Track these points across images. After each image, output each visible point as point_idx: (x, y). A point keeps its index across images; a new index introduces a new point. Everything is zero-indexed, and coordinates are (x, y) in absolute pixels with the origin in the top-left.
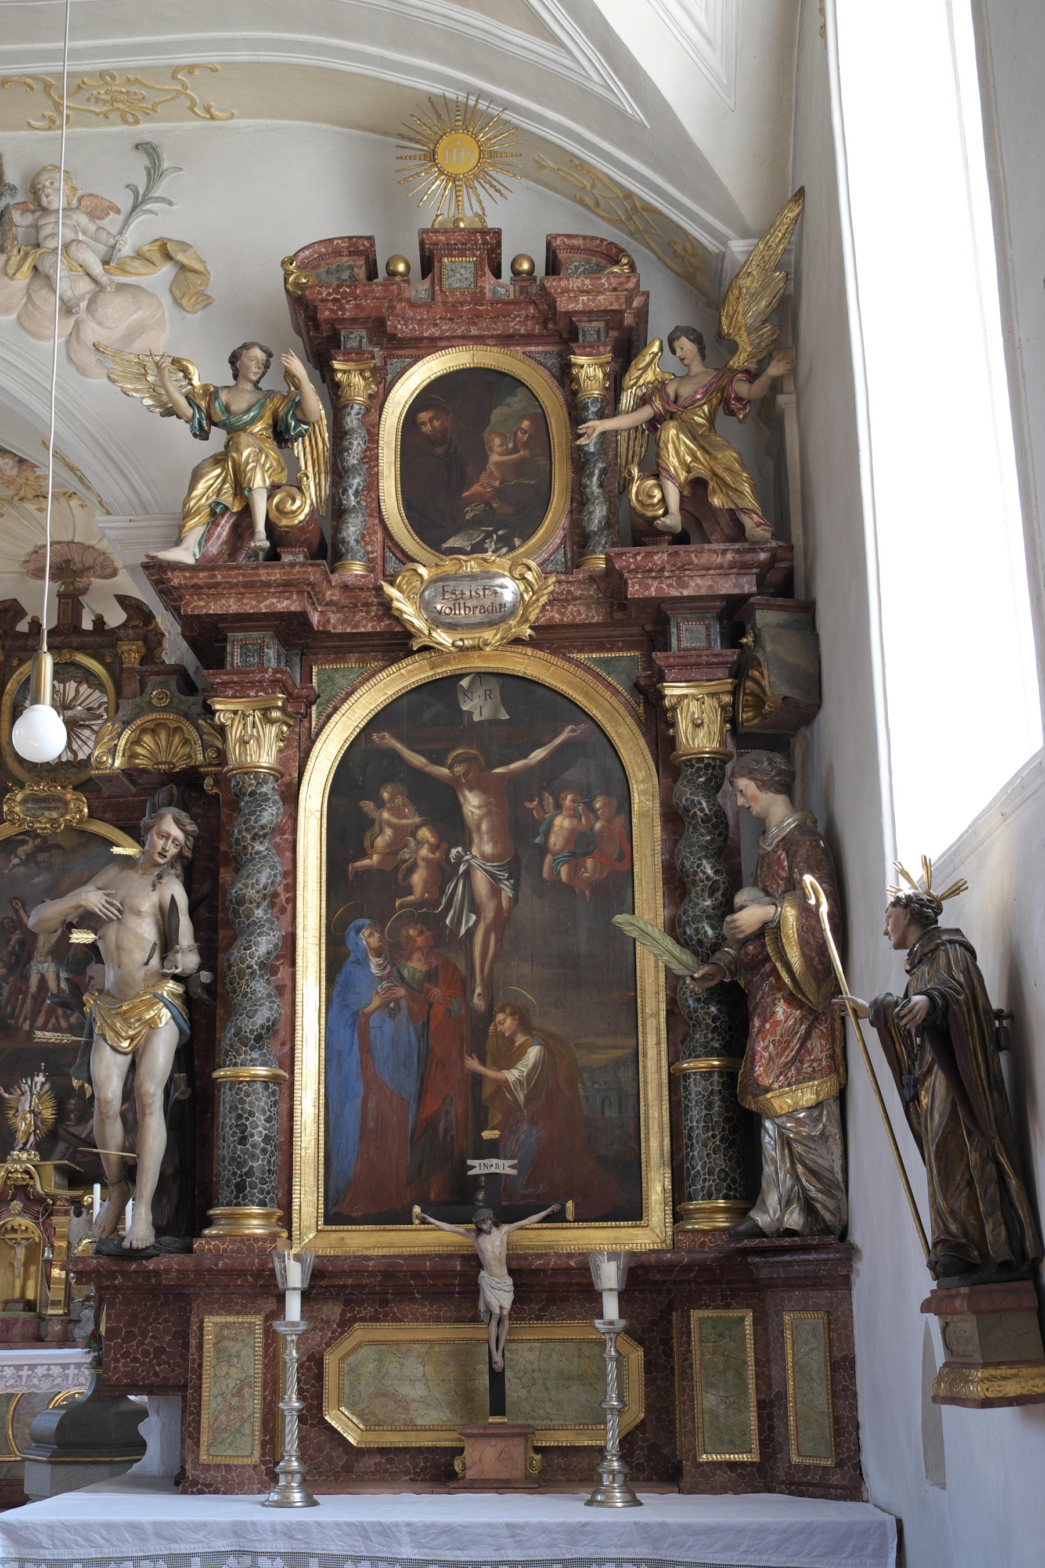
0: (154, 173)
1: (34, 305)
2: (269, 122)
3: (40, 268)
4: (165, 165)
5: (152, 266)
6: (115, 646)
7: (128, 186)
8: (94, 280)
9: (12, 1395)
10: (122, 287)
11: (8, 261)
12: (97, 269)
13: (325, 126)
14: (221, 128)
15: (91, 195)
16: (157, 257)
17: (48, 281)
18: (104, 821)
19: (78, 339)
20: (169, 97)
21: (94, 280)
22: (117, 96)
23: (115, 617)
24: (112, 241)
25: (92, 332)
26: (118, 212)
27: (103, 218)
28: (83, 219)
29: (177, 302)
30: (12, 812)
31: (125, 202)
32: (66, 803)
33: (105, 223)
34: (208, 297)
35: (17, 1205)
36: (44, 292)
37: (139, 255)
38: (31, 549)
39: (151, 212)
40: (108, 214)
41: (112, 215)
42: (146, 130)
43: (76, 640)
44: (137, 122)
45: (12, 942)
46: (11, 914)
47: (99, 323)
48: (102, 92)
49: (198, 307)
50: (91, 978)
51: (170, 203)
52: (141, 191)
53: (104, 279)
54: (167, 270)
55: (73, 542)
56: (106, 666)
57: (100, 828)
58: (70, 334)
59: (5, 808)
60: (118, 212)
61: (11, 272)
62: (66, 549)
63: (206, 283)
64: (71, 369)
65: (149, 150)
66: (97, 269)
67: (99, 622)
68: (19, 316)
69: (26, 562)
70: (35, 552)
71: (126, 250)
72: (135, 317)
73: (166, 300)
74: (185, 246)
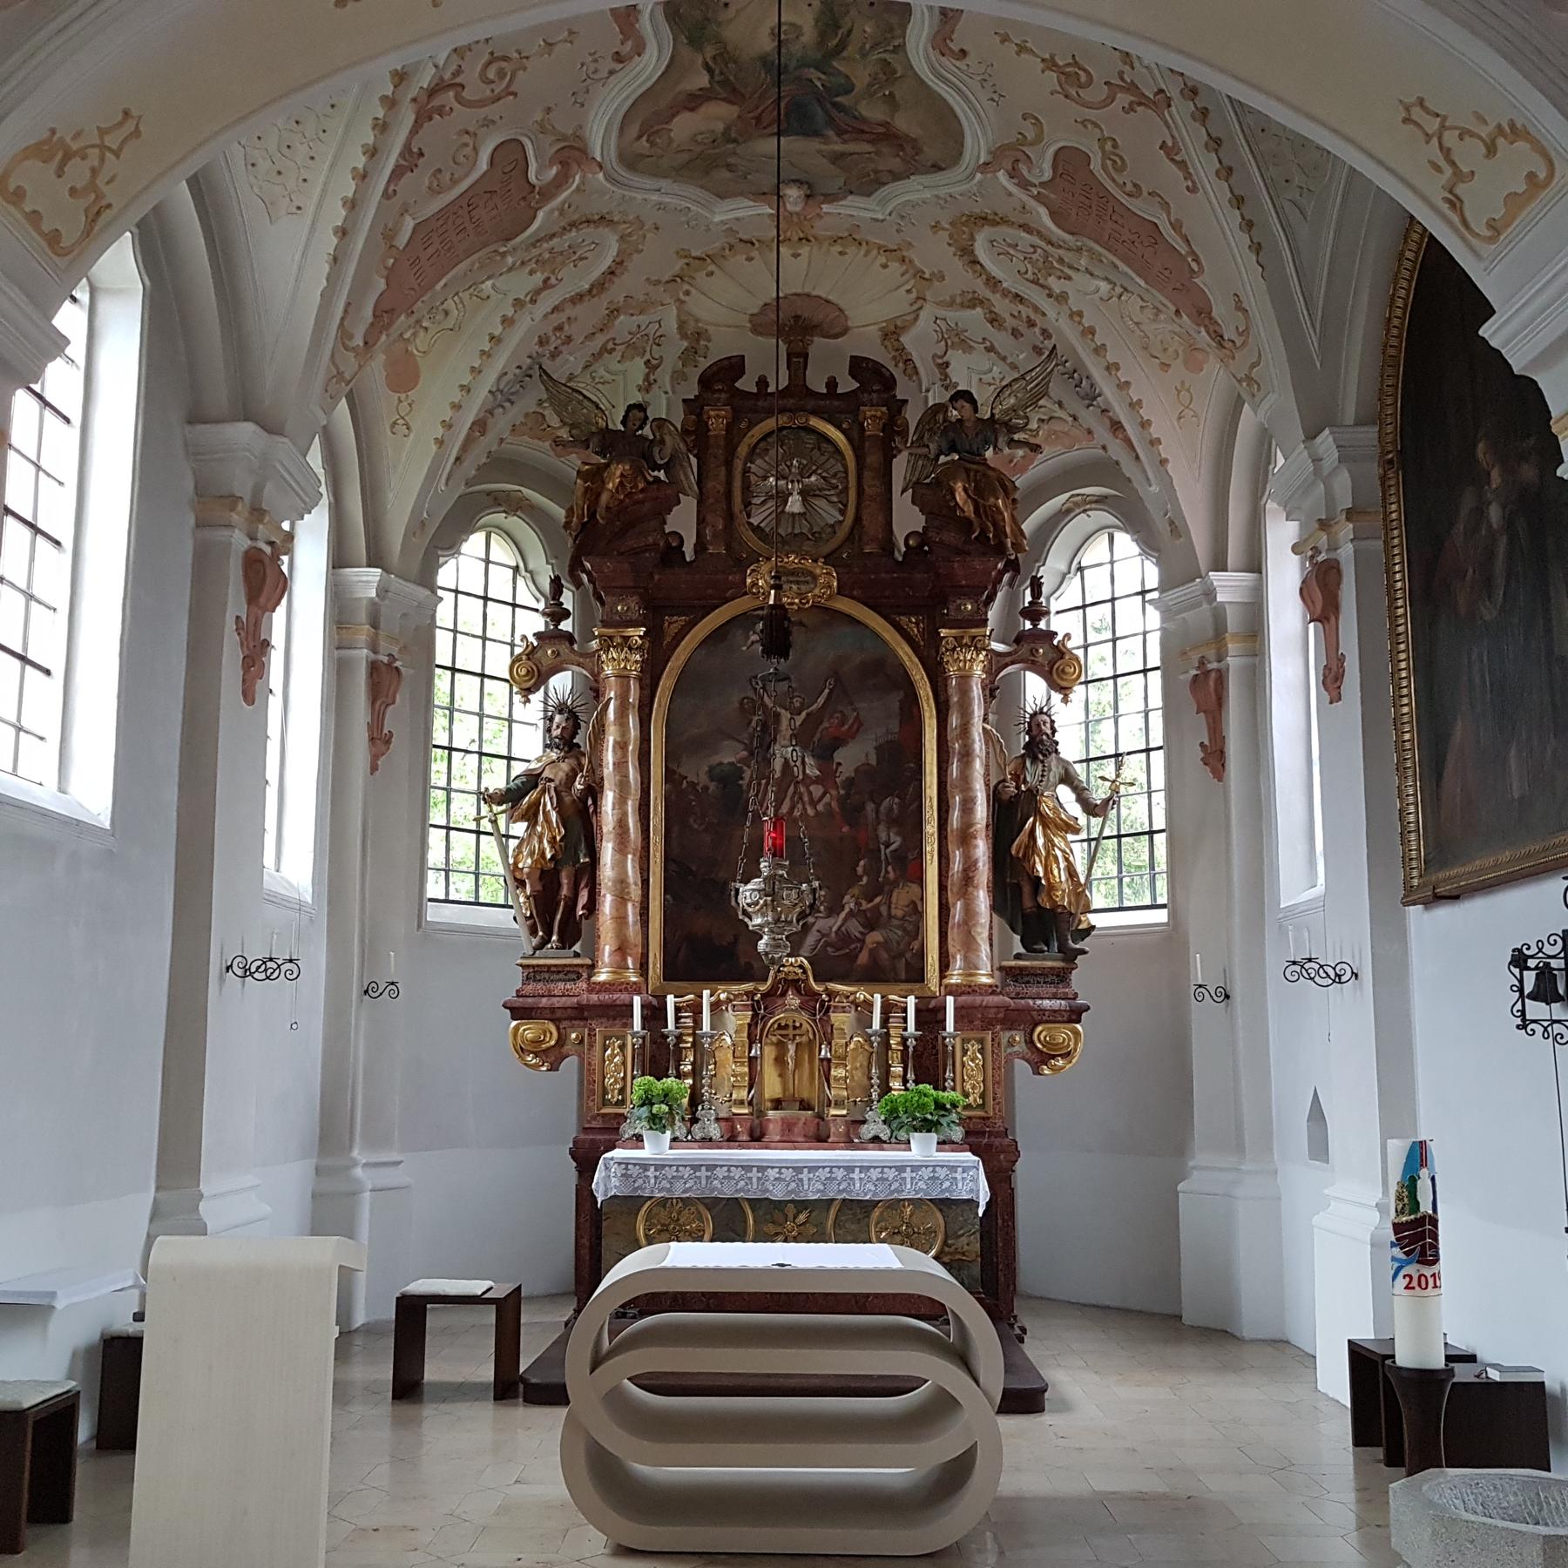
6: (855, 412)
9: (833, 1200)
18: (853, 598)
23: (847, 385)
30: (755, 584)
32: (815, 578)
35: (793, 1000)
43: (811, 404)
45: (754, 724)
46: (751, 694)
50: (839, 764)
56: (843, 432)
57: (845, 605)
59: (749, 581)
67: (832, 384)
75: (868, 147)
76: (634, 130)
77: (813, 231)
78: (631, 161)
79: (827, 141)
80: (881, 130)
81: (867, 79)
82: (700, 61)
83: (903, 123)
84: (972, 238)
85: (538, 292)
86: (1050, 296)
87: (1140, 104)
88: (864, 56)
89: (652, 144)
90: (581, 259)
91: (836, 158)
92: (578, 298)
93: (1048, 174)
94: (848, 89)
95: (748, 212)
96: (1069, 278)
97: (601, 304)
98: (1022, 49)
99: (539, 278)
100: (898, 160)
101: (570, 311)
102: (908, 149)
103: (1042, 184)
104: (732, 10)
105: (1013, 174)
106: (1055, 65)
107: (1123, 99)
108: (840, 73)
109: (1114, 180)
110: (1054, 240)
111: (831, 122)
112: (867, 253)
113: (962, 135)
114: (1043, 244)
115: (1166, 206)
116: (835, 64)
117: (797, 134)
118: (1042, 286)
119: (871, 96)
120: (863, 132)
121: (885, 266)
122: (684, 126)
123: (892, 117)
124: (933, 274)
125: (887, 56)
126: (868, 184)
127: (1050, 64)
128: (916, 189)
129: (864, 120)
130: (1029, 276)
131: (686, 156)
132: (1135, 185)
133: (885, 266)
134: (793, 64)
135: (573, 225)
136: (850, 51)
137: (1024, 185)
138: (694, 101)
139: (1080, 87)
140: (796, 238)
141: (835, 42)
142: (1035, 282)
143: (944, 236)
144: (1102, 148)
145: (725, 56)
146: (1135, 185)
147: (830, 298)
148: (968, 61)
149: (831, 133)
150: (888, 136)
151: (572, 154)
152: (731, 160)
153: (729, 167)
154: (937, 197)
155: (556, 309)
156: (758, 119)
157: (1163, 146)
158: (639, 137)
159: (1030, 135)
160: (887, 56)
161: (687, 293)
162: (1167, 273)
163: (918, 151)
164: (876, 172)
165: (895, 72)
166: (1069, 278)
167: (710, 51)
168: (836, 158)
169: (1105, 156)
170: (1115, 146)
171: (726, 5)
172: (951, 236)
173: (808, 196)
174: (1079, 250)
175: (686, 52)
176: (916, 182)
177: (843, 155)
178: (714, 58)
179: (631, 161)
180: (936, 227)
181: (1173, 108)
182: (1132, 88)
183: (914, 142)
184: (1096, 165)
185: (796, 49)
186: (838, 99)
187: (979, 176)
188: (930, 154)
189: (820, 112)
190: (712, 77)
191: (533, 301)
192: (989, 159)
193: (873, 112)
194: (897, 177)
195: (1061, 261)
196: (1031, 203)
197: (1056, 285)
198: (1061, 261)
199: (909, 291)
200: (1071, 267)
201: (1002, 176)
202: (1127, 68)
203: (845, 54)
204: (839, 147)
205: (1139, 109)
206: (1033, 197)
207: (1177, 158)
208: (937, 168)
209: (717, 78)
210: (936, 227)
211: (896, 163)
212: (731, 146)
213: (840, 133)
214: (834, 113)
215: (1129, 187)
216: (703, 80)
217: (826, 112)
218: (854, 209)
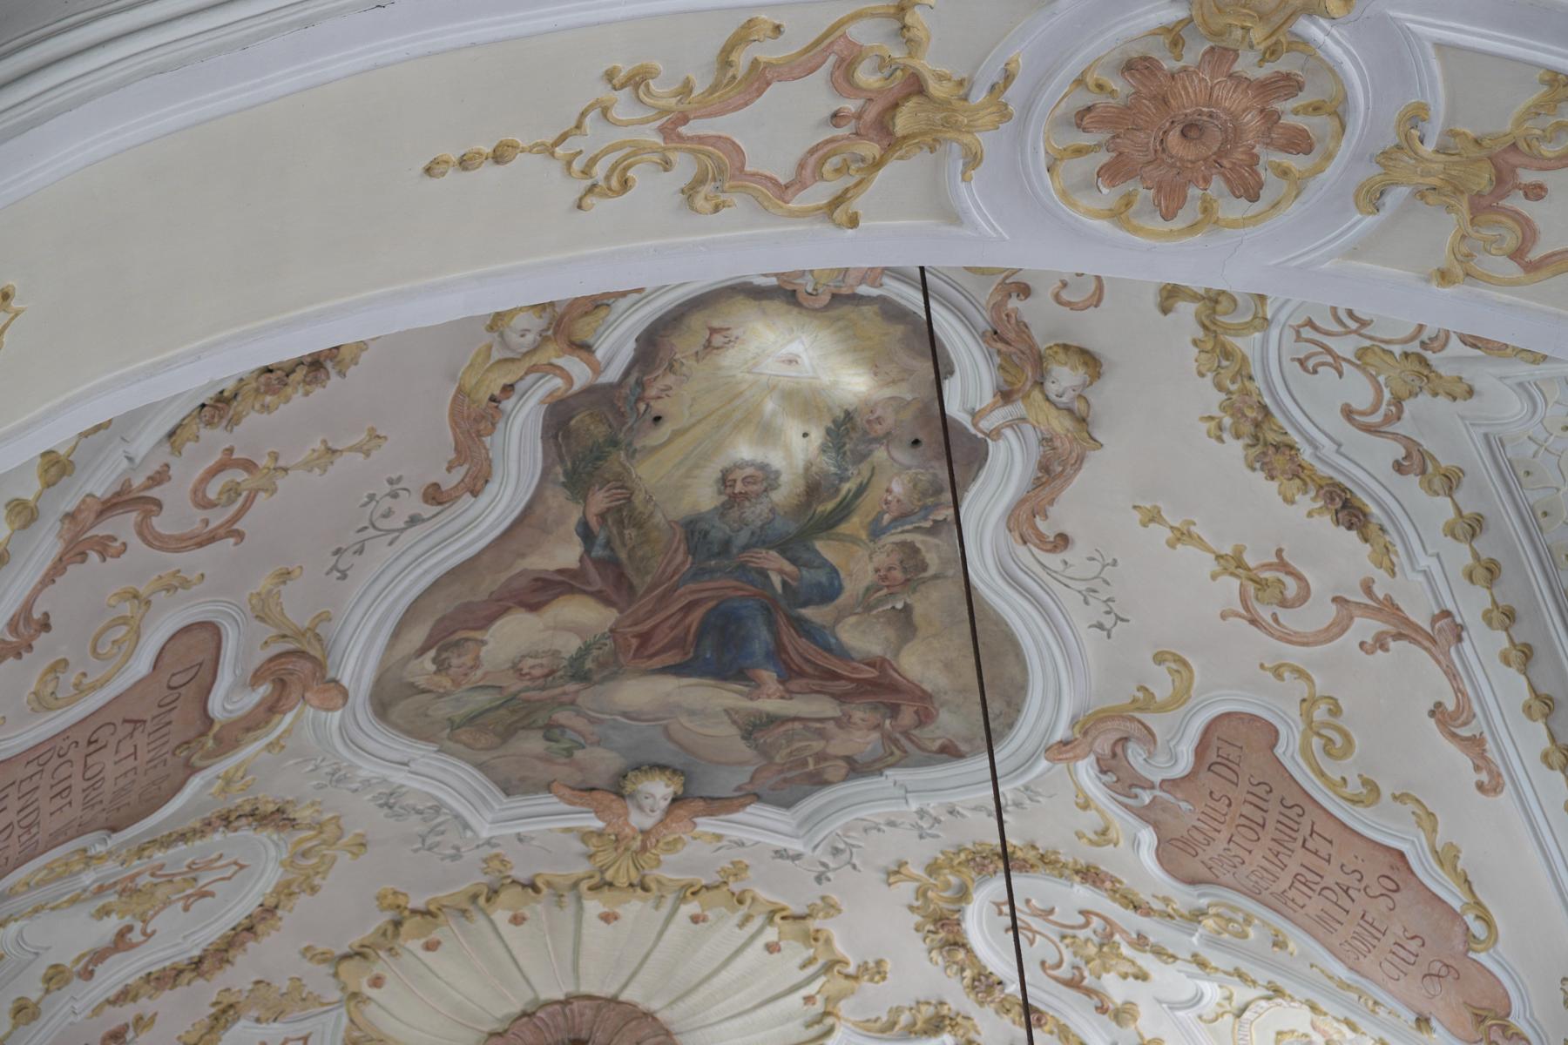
38: (516, 1007)
55: (613, 1001)
62: (589, 1013)
69: (492, 1035)
70: (524, 1014)
76: (417, 635)
77: (657, 872)
78: (390, 699)
80: (870, 673)
81: (869, 578)
82: (575, 516)
83: (915, 665)
84: (963, 894)
85: (99, 956)
86: (1102, 1009)
87: (1399, 636)
88: (876, 531)
89: (441, 666)
90: (203, 895)
91: (754, 727)
92: (168, 978)
94: (828, 592)
95: (550, 828)
96: (1142, 976)
97: (203, 994)
98: (1183, 535)
99: (113, 924)
100: (875, 735)
101: (145, 1006)
103: (1171, 784)
104: (666, 430)
106: (1240, 564)
107: (1366, 627)
108: (825, 564)
109: (1321, 774)
110: (1144, 896)
111: (778, 656)
115: (1428, 820)
116: (819, 545)
117: (702, 674)
118: (1089, 992)
119: (869, 609)
120: (835, 676)
121: (771, 948)
122: (514, 637)
123: (897, 653)
124: (864, 967)
125: (917, 539)
127: (1233, 563)
129: (843, 654)
130: (1065, 972)
131: (482, 700)
132: (1366, 782)
133: (771, 948)
134: (743, 538)
135: (227, 820)
136: (854, 525)
137: (1124, 782)
138: (540, 592)
139: (1283, 603)
140: (622, 881)
141: (830, 506)
142: (1074, 984)
143: (906, 890)
144: (1307, 716)
145: (624, 514)
146: (1366, 782)
147: (654, 1005)
148: (1066, 555)
149: (768, 676)
150: (882, 688)
151: (296, 670)
152: (562, 717)
153: (551, 731)
155: (125, 995)
156: (645, 638)
157: (1437, 711)
158: (422, 651)
159: (1162, 688)
160: (917, 539)
161: (377, 982)
162: (1413, 946)
165: (925, 568)
166: (1142, 976)
167: (599, 500)
168: (754, 727)
169: (1311, 728)
170: (1335, 710)
171: (657, 419)
172: (922, 893)
174: (1197, 916)
175: (557, 499)
177: (773, 720)
178: (602, 516)
179: (390, 699)
180: (895, 872)
181: (1466, 645)
182: (1388, 609)
184: (1288, 749)
185: (756, 512)
186: (808, 612)
187: (1044, 764)
188: (953, 722)
189: (764, 634)
190: (588, 551)
191: (88, 974)
193: (862, 638)
194: (856, 769)
195: (1141, 942)
197: (1116, 988)
198: (1141, 942)
199: (809, 1000)
200: (1159, 952)
201: (1085, 771)
202: (1380, 575)
203: (844, 528)
204: (771, 704)
205: (1392, 644)
207: (1464, 732)
209: (598, 552)
210: (895, 872)
211: (863, 742)
212: (572, 687)
213: (789, 673)
214: (789, 636)
215: (1355, 787)
216: (567, 554)
217: (776, 636)
218: (760, 828)
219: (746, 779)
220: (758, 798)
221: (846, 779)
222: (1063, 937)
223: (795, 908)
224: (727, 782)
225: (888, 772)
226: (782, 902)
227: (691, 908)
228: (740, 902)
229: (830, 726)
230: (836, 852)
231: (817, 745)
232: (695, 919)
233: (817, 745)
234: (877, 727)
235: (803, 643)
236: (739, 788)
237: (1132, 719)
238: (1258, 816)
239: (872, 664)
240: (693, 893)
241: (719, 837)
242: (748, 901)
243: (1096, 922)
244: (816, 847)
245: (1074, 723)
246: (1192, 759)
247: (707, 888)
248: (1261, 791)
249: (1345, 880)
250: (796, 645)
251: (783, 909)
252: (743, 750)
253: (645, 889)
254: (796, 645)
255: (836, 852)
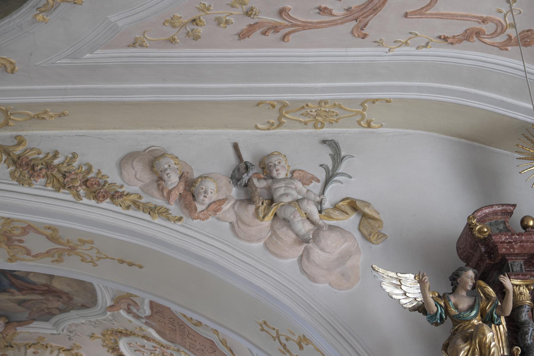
0: (337, 158)
1: (278, 237)
2: (401, 130)
3: (278, 214)
4: (343, 154)
5: (346, 215)
7: (321, 165)
8: (313, 222)
10: (331, 228)
11: (257, 209)
12: (316, 216)
13: (435, 134)
14: (372, 132)
15: (300, 170)
16: (348, 209)
17: (287, 223)
19: (308, 258)
20: (350, 115)
21: (313, 222)
22: (320, 113)
24: (318, 199)
25: (317, 254)
26: (318, 181)
27: (308, 185)
28: (299, 185)
29: (366, 238)
31: (322, 175)
33: (311, 187)
34: (385, 235)
36: (285, 229)
37: (335, 207)
39: (340, 182)
40: (311, 182)
41: (314, 182)
42: (328, 132)
44: (322, 127)
47: (322, 250)
48: (314, 110)
49: (379, 240)
51: (350, 177)
52: (331, 168)
53: (321, 222)
54: (354, 218)
58: (301, 256)
60: (318, 181)
61: (261, 216)
63: (381, 226)
64: (304, 277)
65: (333, 145)
66: (316, 216)
68: (265, 244)
71: (327, 205)
72: (344, 246)
73: (357, 235)
74: (368, 204)
75: (40, 297)
79: (12, 294)
80: (46, 288)
83: (56, 285)
84: (116, 342)
91: (21, 303)
93: (148, 312)
100: (60, 303)
102: (65, 298)
103: (147, 317)
105: (129, 311)
111: (12, 285)
112: (52, 352)
113: (94, 290)
114: (158, 346)
126: (46, 315)
128: (74, 319)
129: (34, 284)
143: (99, 341)
149: (13, 290)
154: (90, 321)
163: (71, 299)
164: (48, 309)
173: (7, 323)
176: (73, 313)
177: (24, 301)
180: (92, 336)
183: (66, 294)
187: (109, 313)
188: (78, 300)
192: (112, 303)
194: (62, 311)
196: (144, 327)
201: (123, 313)
206: (144, 323)
208: (84, 307)
211: (59, 304)
213: (20, 290)
214: (13, 280)
218: (39, 329)
219: (28, 315)
220: (35, 320)
221: (60, 313)
222: (151, 353)
223: (66, 347)
224: (25, 316)
225: (72, 311)
226: (62, 346)
227: (30, 351)
228: (47, 347)
229: (44, 301)
230: (70, 332)
231: (45, 306)
232: (34, 353)
233: (45, 306)
234: (59, 301)
235: (19, 281)
236: (27, 318)
237: (129, 299)
238: (173, 327)
239: (44, 286)
240: (29, 346)
241: (29, 332)
242: (49, 347)
243: (158, 349)
244: (63, 331)
245: (112, 299)
246: (150, 311)
247: (34, 344)
248: (172, 320)
249: (203, 348)
250: (18, 282)
251: (62, 348)
252: (19, 308)
253: (12, 347)
254: (18, 282)
255: (70, 332)
